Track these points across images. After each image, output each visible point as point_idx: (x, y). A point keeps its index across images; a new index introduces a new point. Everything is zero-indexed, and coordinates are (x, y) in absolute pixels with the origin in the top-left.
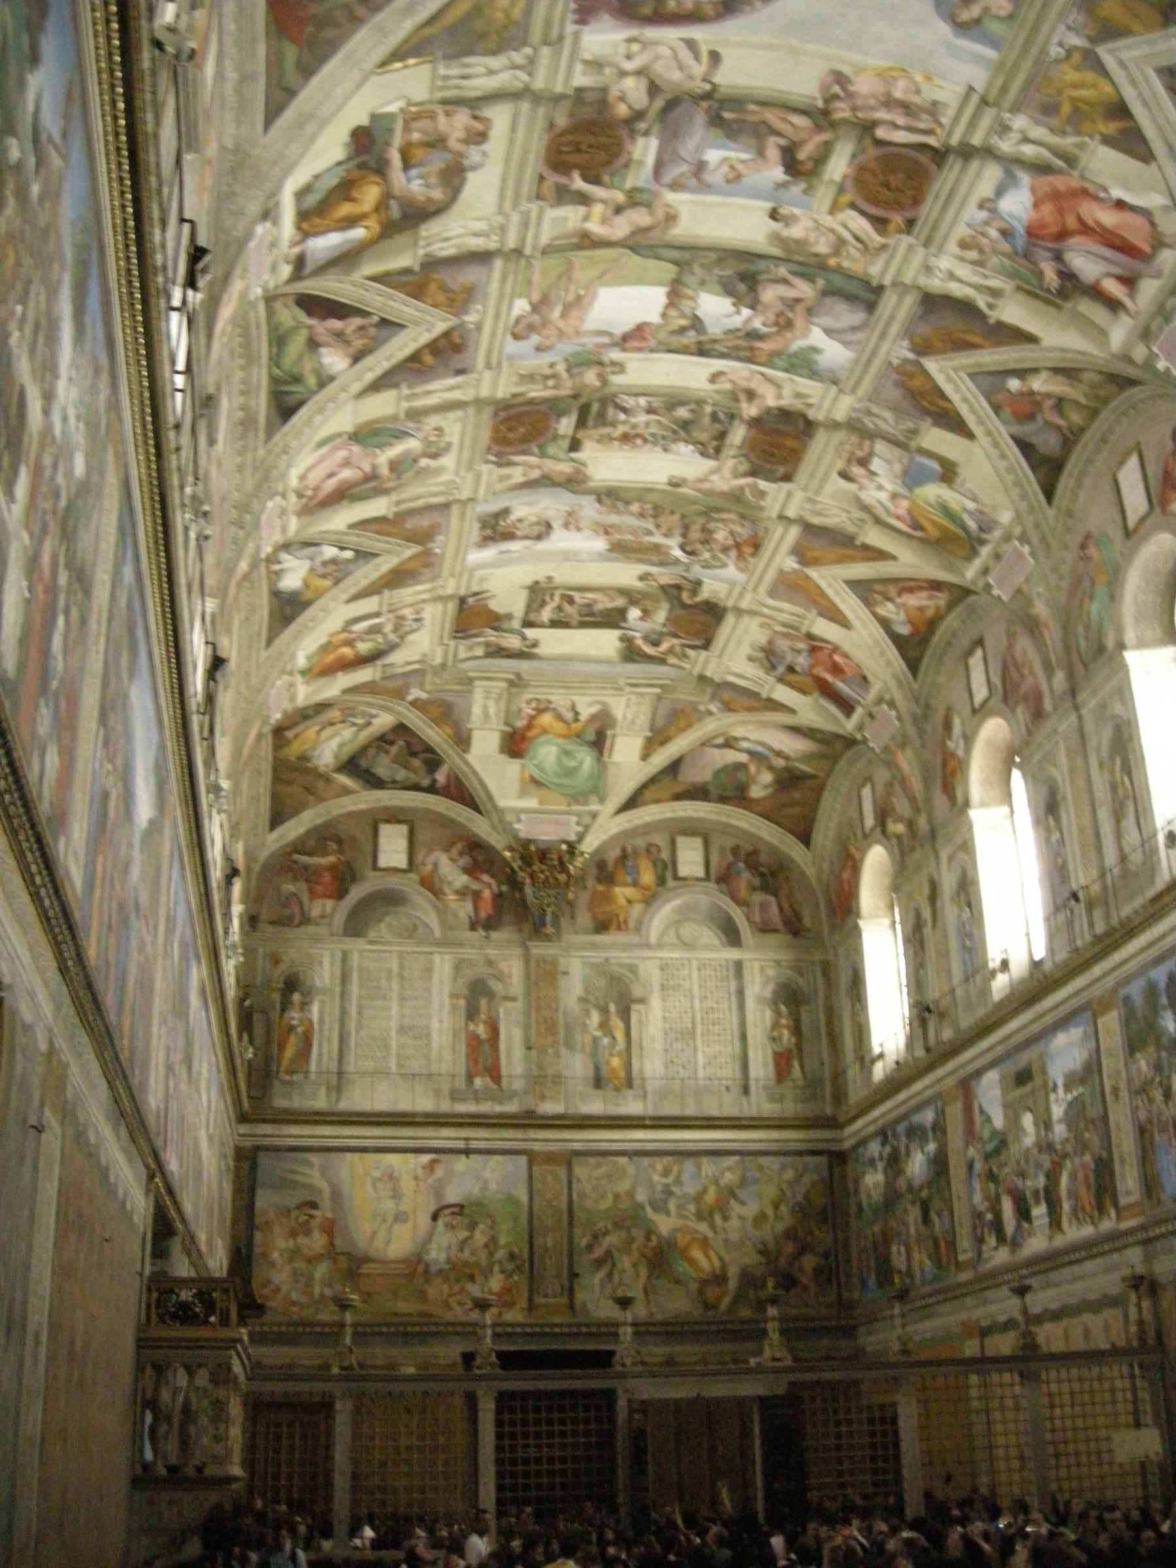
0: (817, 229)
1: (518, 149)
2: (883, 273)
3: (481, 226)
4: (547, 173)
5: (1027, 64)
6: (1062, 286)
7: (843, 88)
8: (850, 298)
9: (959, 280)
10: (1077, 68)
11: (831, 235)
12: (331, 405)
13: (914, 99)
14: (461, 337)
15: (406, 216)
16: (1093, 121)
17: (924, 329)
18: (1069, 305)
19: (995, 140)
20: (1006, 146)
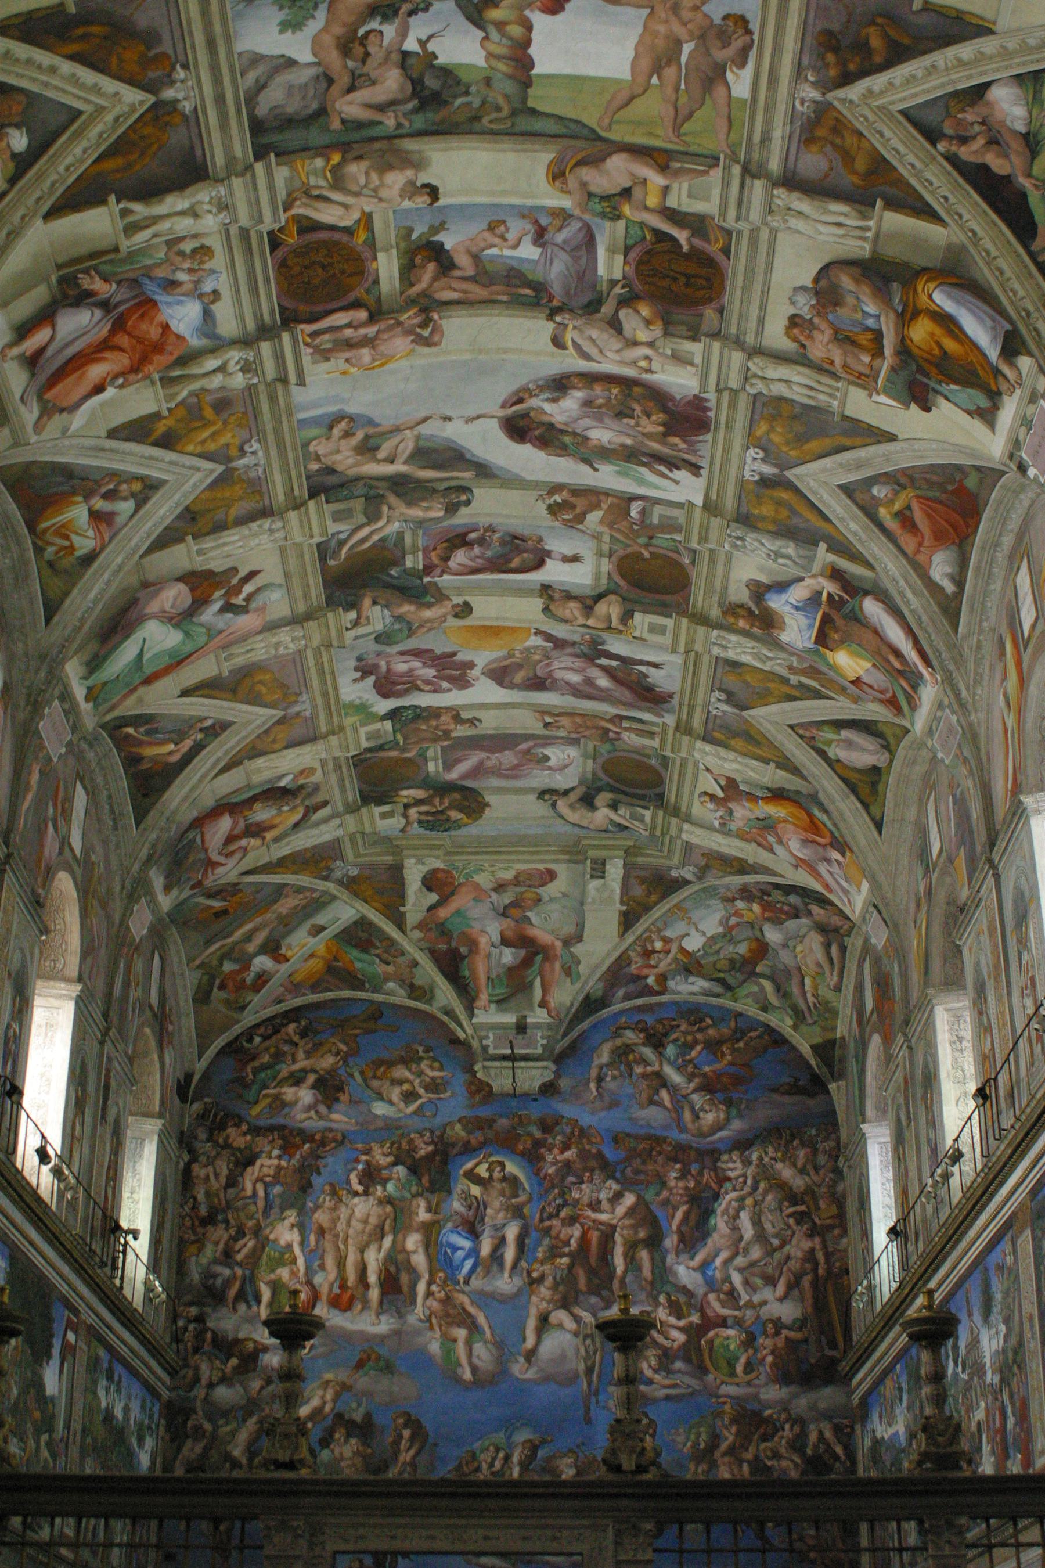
0: (375, 190)
1: (756, 297)
2: (270, 175)
3: (794, 223)
4: (720, 258)
5: (269, 428)
6: (78, 285)
7: (419, 335)
8: (289, 122)
9: (182, 213)
10: (228, 445)
11: (355, 189)
12: (1032, 42)
13: (348, 355)
14: (827, 66)
15: (887, 280)
16: (178, 421)
17: (177, 137)
18: (54, 279)
19: (251, 355)
20: (235, 356)
